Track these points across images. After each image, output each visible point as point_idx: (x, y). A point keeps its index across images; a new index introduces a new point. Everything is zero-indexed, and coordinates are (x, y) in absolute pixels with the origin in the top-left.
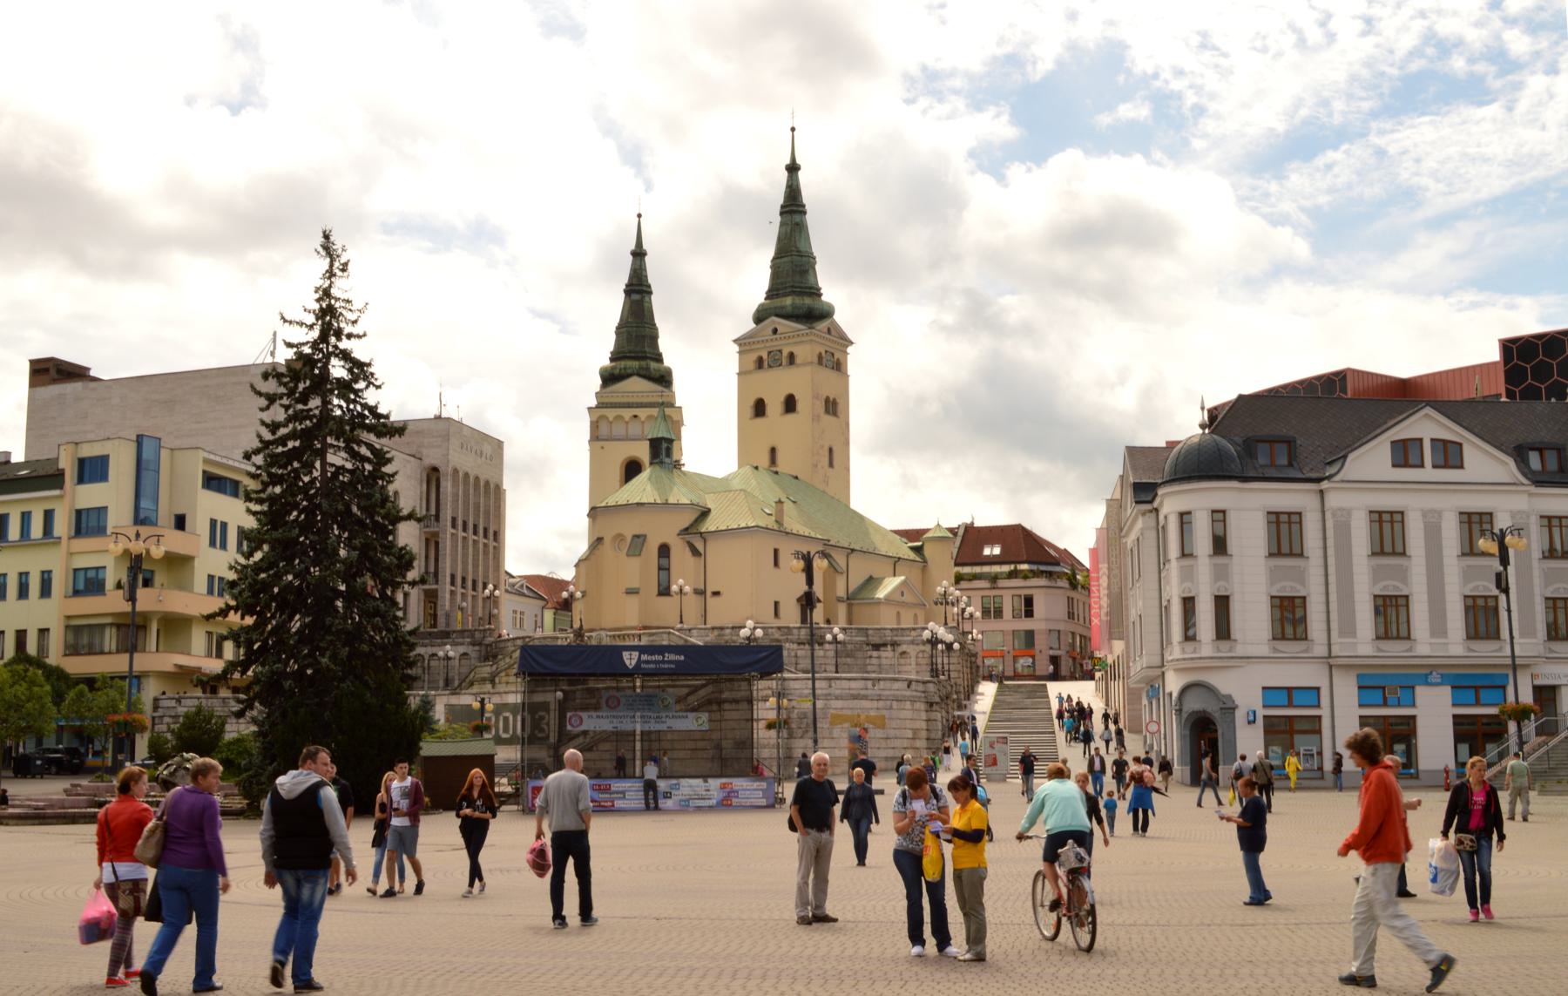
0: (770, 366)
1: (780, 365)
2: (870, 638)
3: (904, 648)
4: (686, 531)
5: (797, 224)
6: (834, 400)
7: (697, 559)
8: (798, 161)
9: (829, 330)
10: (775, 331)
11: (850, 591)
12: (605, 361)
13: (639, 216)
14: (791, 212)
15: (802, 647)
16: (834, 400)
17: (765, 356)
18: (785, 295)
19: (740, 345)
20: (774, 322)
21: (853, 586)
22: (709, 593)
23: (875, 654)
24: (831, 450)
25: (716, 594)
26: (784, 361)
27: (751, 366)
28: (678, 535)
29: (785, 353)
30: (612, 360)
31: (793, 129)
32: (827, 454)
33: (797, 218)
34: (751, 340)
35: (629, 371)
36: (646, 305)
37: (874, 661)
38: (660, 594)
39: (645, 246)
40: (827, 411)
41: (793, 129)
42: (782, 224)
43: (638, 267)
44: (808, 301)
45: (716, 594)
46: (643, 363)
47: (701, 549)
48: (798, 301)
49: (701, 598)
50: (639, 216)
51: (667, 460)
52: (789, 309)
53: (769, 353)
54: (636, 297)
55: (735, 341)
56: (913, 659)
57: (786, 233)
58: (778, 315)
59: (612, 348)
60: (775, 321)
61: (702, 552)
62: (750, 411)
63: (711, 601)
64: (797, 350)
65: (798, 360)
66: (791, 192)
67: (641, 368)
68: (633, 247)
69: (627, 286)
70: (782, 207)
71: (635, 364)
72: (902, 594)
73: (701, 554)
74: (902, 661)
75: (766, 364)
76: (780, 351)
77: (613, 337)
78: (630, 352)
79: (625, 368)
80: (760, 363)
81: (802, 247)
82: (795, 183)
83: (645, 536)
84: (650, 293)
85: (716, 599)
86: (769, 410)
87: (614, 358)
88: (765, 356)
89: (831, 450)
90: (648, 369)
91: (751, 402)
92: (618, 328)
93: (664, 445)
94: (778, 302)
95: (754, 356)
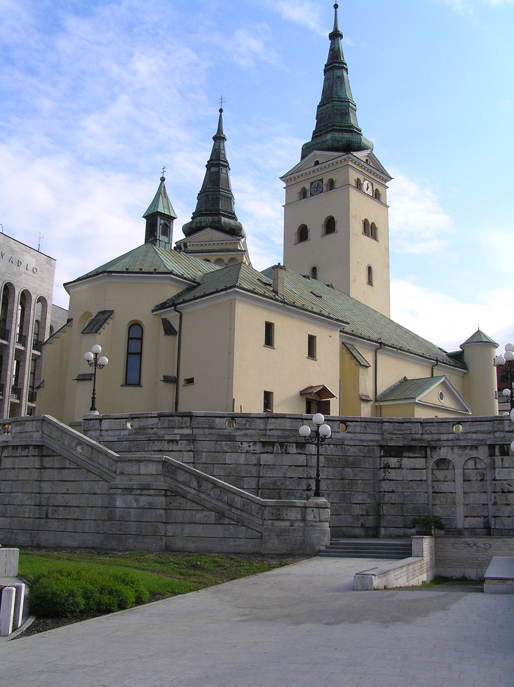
0: (312, 195)
1: (321, 193)
2: (386, 436)
3: (443, 453)
4: (163, 306)
5: (339, 77)
6: (373, 224)
7: (170, 338)
8: (341, 29)
9: (367, 160)
10: (317, 163)
11: (378, 394)
13: (221, 111)
15: (270, 449)
16: (373, 224)
17: (308, 187)
18: (326, 133)
19: (286, 181)
21: (383, 387)
22: (182, 382)
23: (393, 461)
24: (370, 269)
25: (190, 381)
27: (296, 197)
28: (153, 311)
29: (325, 181)
31: (336, 6)
32: (366, 273)
33: (338, 73)
34: (298, 174)
35: (203, 224)
36: (222, 175)
37: (392, 474)
38: (127, 384)
39: (225, 133)
40: (365, 232)
41: (336, 6)
43: (216, 148)
44: (346, 135)
45: (190, 381)
46: (216, 218)
47: (176, 326)
48: (337, 135)
49: (171, 387)
50: (221, 111)
51: (162, 238)
52: (329, 143)
53: (312, 183)
54: (214, 169)
55: (281, 178)
56: (459, 472)
58: (318, 150)
60: (318, 155)
61: (177, 330)
62: (294, 238)
63: (184, 391)
65: (337, 185)
66: (333, 53)
67: (213, 221)
70: (326, 66)
71: (210, 219)
72: (441, 396)
74: (440, 474)
75: (309, 194)
76: (321, 180)
77: (195, 202)
78: (206, 210)
79: (200, 222)
80: (304, 194)
82: (336, 46)
83: (112, 312)
84: (227, 167)
85: (190, 387)
86: (311, 234)
87: (196, 215)
88: (308, 187)
89: (370, 269)
90: (220, 221)
91: (296, 229)
92: (199, 195)
93: (160, 222)
94: (319, 140)
95: (299, 189)
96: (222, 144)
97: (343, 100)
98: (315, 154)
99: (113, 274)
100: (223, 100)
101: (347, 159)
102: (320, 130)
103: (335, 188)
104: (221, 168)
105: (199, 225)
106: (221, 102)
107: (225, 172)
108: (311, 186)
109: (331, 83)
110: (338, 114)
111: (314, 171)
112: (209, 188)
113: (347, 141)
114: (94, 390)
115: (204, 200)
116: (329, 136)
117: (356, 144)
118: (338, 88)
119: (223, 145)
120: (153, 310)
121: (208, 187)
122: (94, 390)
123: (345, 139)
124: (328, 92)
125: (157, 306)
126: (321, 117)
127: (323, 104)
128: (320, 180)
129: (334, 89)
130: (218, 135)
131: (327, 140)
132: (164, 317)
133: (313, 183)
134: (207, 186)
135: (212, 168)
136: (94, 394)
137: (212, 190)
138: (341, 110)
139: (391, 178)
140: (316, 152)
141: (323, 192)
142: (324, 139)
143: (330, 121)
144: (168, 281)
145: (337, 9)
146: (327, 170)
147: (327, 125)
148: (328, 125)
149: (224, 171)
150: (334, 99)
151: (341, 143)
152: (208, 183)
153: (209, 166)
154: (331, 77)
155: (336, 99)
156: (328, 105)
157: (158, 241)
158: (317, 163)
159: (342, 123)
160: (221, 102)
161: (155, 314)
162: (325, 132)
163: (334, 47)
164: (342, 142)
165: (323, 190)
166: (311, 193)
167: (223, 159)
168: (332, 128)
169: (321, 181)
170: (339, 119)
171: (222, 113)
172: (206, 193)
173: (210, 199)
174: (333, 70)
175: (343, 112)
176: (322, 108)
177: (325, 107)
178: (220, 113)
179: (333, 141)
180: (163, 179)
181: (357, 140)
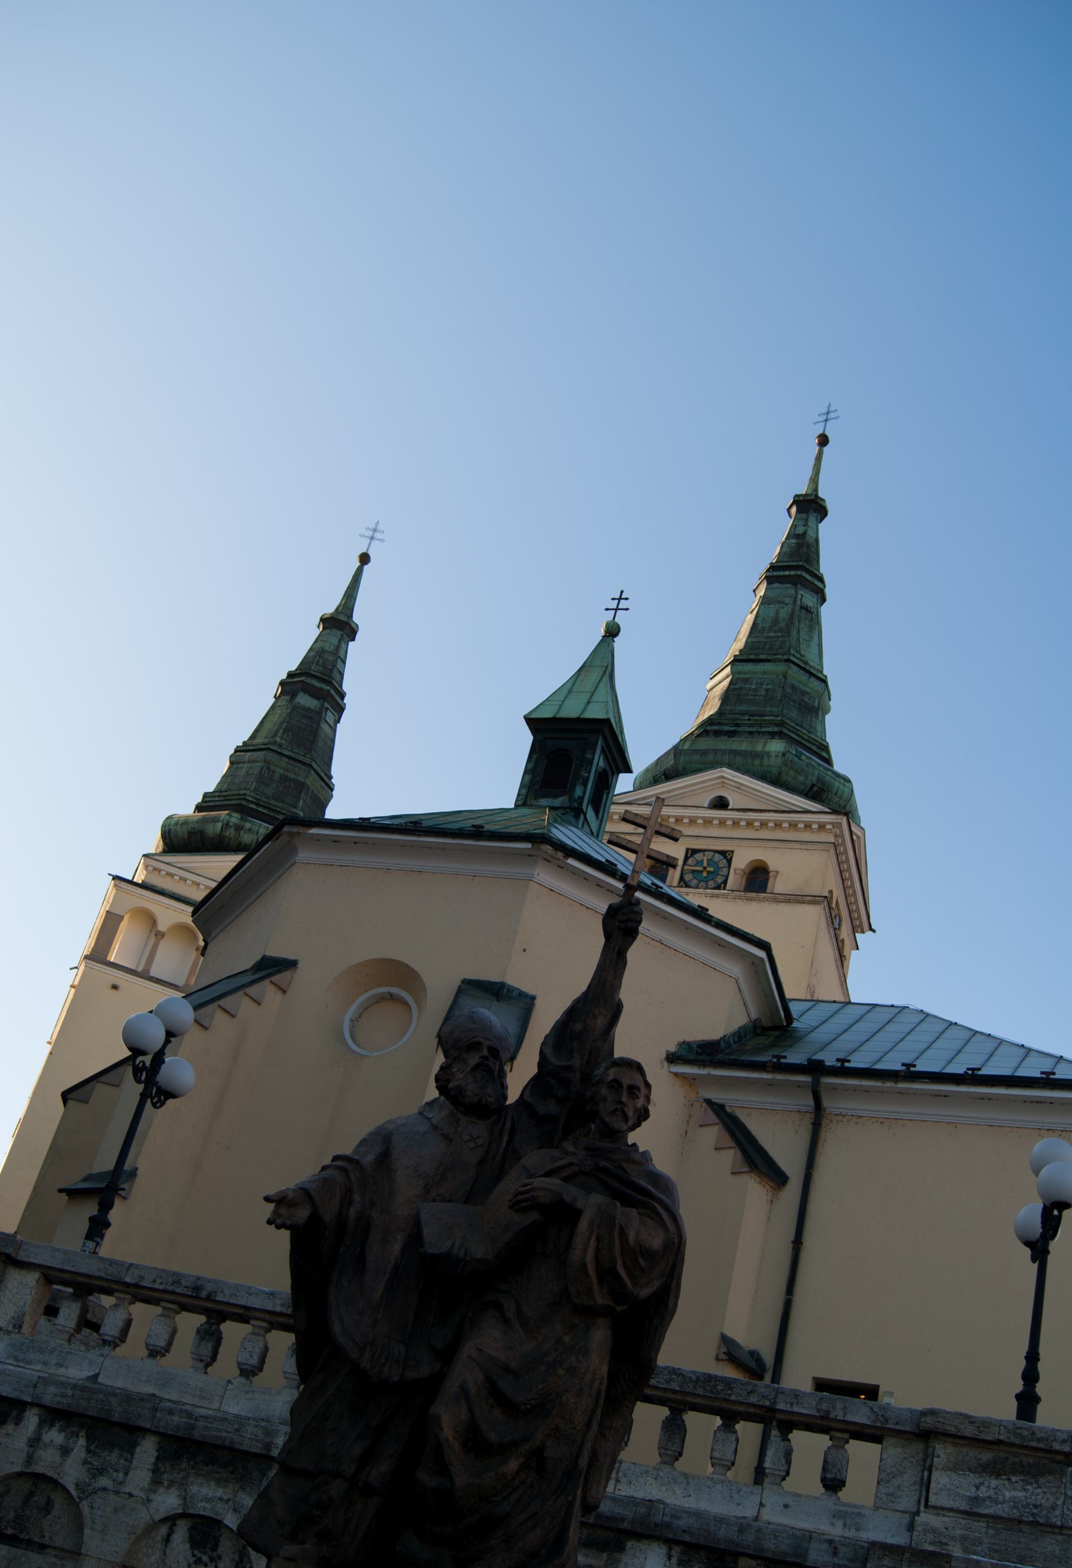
1: (718, 887)
5: (806, 609)
10: (721, 803)
12: (186, 807)
13: (365, 559)
14: (796, 582)
18: (773, 735)
20: (723, 781)
26: (734, 880)
29: (742, 860)
30: (199, 808)
31: (823, 441)
41: (823, 441)
42: (765, 601)
50: (365, 559)
52: (774, 762)
54: (305, 700)
57: (776, 620)
59: (211, 788)
64: (773, 859)
65: (778, 885)
66: (799, 546)
68: (330, 608)
69: (290, 675)
73: (776, 1177)
76: (727, 856)
79: (239, 828)
81: (811, 656)
83: (533, 998)
84: (340, 710)
96: (343, 646)
97: (812, 671)
98: (723, 777)
99: (571, 861)
100: (377, 535)
101: (829, 827)
102: (735, 719)
103: (769, 890)
104: (326, 705)
105: (231, 832)
106: (372, 538)
107: (332, 724)
108: (686, 858)
109: (784, 613)
110: (794, 701)
111: (708, 822)
112: (280, 746)
113: (818, 779)
114: (1033, 1357)
115: (256, 771)
116: (776, 746)
117: (836, 799)
118: (803, 635)
119: (345, 650)
120: (673, 1054)
121: (278, 739)
122: (1033, 1357)
123: (816, 772)
124: (771, 634)
125: (685, 1045)
126: (741, 688)
127: (752, 657)
128: (723, 853)
129: (794, 633)
130: (342, 618)
131: (768, 754)
132: (717, 1096)
133: (695, 851)
134: (275, 735)
135: (301, 694)
136: (1031, 1376)
137: (288, 753)
138: (804, 693)
139: (871, 929)
140: (727, 772)
141: (724, 888)
142: (759, 748)
143: (768, 709)
144: (735, 969)
145: (825, 449)
146: (806, 836)
147: (763, 715)
148: (764, 718)
149: (330, 717)
150: (792, 658)
151: (802, 778)
152: (281, 731)
153: (291, 685)
154: (787, 600)
155: (796, 660)
156: (768, 667)
157: (582, 817)
158: (721, 803)
159: (801, 726)
160: (372, 538)
161: (676, 1074)
162: (750, 729)
163: (805, 533)
164: (806, 777)
165: (725, 882)
166: (682, 879)
167: (336, 685)
168: (776, 729)
169: (725, 857)
170: (794, 713)
171: (365, 567)
172: (270, 756)
173: (276, 777)
174: (795, 584)
175: (806, 700)
176: (749, 667)
177: (760, 667)
178: (358, 564)
179: (786, 764)
180: (612, 632)
181: (842, 787)
